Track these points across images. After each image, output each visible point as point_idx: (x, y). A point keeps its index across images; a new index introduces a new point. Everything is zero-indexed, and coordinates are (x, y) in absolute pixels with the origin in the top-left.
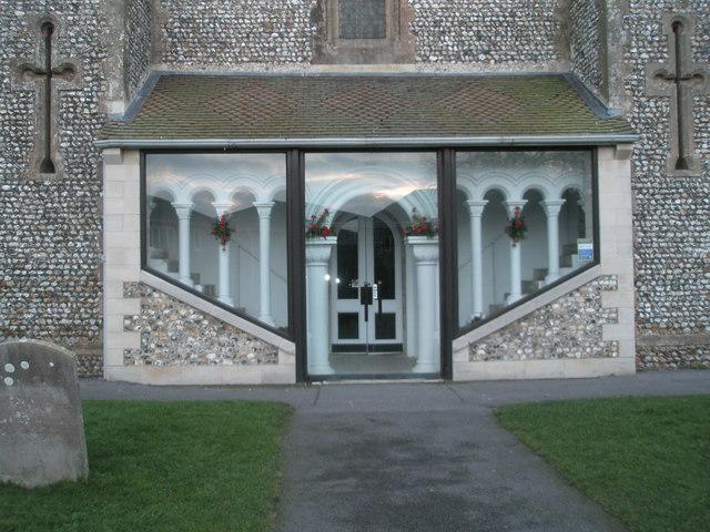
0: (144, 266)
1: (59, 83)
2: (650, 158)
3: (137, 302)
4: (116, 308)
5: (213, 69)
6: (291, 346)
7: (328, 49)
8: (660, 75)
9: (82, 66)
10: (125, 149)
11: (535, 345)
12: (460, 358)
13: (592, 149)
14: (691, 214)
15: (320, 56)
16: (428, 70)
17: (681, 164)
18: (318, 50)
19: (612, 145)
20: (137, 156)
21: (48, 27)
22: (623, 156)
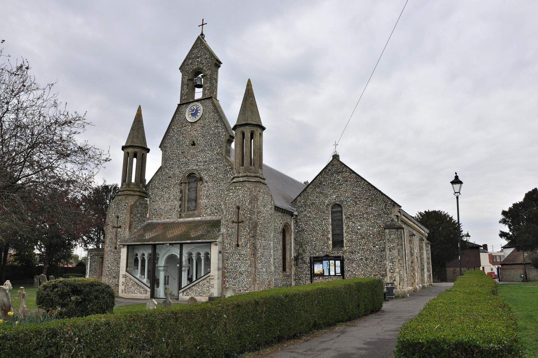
0: (127, 271)
1: (119, 229)
2: (230, 244)
4: (122, 280)
5: (159, 221)
6: (149, 290)
7: (183, 215)
8: (233, 222)
10: (124, 245)
11: (196, 293)
12: (181, 295)
13: (210, 243)
14: (239, 259)
15: (181, 217)
16: (204, 219)
18: (180, 215)
19: (213, 242)
21: (118, 217)
22: (216, 245)
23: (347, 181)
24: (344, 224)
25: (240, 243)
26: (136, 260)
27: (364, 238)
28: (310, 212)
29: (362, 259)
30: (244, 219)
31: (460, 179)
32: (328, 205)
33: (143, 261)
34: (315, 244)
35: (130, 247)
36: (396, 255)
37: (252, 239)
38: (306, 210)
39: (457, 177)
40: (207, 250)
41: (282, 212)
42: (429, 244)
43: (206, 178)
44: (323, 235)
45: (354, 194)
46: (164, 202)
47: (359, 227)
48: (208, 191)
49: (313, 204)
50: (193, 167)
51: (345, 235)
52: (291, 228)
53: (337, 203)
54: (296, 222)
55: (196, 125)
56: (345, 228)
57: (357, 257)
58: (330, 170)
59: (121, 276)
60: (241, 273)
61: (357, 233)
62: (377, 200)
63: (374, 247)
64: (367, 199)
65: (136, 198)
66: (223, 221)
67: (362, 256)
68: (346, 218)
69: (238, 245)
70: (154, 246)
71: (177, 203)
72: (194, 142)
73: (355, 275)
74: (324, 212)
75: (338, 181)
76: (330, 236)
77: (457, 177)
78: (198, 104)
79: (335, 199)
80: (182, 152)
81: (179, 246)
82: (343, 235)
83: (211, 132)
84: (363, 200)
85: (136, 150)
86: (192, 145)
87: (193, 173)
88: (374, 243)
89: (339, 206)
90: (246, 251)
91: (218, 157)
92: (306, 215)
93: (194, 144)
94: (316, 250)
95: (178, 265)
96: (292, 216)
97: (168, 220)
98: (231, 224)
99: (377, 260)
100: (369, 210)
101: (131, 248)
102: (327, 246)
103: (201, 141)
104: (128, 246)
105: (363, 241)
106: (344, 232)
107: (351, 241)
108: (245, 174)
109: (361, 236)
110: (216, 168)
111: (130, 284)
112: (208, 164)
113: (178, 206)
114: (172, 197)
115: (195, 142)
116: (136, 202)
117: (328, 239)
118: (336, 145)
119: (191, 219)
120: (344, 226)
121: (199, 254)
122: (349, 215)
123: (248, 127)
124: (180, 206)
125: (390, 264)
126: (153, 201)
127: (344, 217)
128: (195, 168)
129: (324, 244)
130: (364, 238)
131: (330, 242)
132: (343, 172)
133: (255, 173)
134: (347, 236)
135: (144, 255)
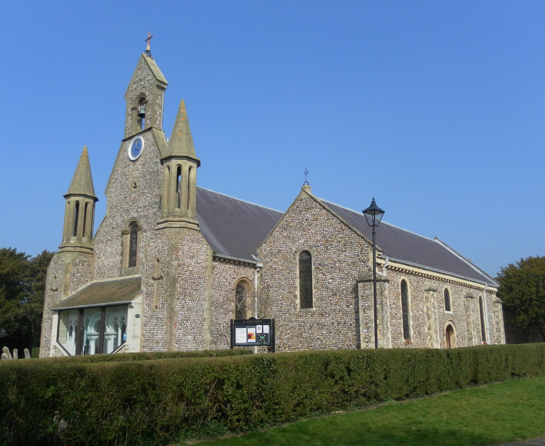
3: (54, 350)
5: (103, 281)
7: (123, 272)
9: (59, 289)
10: (55, 311)
15: (121, 275)
20: (57, 312)
23: (316, 220)
24: (313, 276)
27: (336, 295)
28: (276, 263)
29: (333, 323)
30: (163, 275)
31: (379, 205)
32: (296, 252)
34: (281, 304)
35: (62, 312)
37: (169, 299)
38: (271, 260)
39: (373, 203)
41: (235, 265)
42: (498, 302)
43: (145, 227)
44: (289, 293)
45: (325, 237)
46: (108, 257)
47: (330, 281)
48: (146, 242)
49: (280, 251)
51: (314, 291)
52: (253, 284)
53: (306, 249)
54: (261, 276)
55: (138, 163)
56: (314, 282)
57: (327, 320)
58: (297, 207)
60: (157, 342)
61: (328, 288)
62: (351, 243)
64: (340, 242)
65: (76, 254)
66: (143, 278)
68: (316, 268)
71: (119, 258)
73: (326, 344)
74: (291, 262)
75: (306, 220)
76: (298, 293)
77: (373, 203)
78: (141, 137)
79: (303, 245)
82: (312, 291)
83: (151, 170)
87: (134, 222)
88: (348, 301)
89: (307, 253)
90: (163, 314)
94: (281, 311)
96: (256, 268)
97: (110, 279)
98: (152, 281)
99: (351, 325)
100: (342, 257)
102: (294, 306)
103: (141, 183)
105: (335, 300)
106: (313, 286)
110: (154, 214)
112: (148, 209)
116: (74, 260)
117: (295, 296)
118: (306, 173)
119: (130, 277)
120: (313, 280)
122: (319, 264)
123: (173, 160)
125: (365, 330)
126: (98, 258)
127: (313, 267)
128: (136, 215)
129: (291, 304)
130: (336, 295)
131: (298, 301)
132: (312, 208)
133: (180, 217)
134: (316, 292)
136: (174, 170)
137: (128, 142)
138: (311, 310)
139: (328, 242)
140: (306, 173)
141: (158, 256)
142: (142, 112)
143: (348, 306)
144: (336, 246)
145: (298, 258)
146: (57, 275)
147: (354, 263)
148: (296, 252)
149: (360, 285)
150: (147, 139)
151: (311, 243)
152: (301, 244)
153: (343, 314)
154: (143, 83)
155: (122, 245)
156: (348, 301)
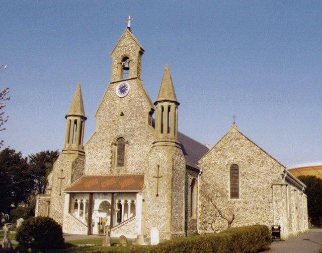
10: (67, 193)
12: (112, 233)
17: (157, 195)
19: (138, 192)
22: (141, 194)
23: (242, 146)
25: (159, 194)
26: (76, 205)
28: (213, 170)
32: (228, 165)
33: (82, 205)
36: (281, 206)
40: (133, 198)
41: (191, 169)
49: (215, 164)
50: (121, 133)
51: (240, 189)
53: (235, 163)
56: (240, 184)
57: (250, 206)
59: (64, 217)
60: (159, 217)
63: (264, 199)
67: (254, 206)
69: (157, 195)
70: (91, 194)
71: (109, 161)
72: (122, 113)
73: (248, 221)
76: (229, 189)
80: (113, 121)
81: (111, 195)
84: (255, 162)
85: (76, 118)
86: (121, 115)
88: (264, 196)
91: (141, 125)
92: (209, 172)
93: (122, 114)
95: (110, 210)
98: (152, 179)
100: (261, 169)
101: (72, 195)
104: (70, 193)
105: (255, 194)
107: (245, 194)
108: (164, 140)
109: (254, 190)
111: (72, 223)
113: (109, 163)
114: (104, 156)
115: (124, 113)
117: (227, 191)
121: (126, 201)
124: (111, 163)
128: (123, 133)
130: (256, 191)
135: (82, 201)
136: (166, 109)
137: (115, 84)
138: (238, 200)
139: (250, 161)
140: (234, 117)
141: (158, 163)
142: (126, 66)
143: (264, 199)
144: (256, 163)
145: (229, 168)
146: (64, 169)
147: (268, 174)
148: (228, 165)
149: (274, 186)
150: (132, 84)
151: (239, 160)
152: (231, 159)
153: (261, 203)
154: (127, 48)
155: (112, 152)
156: (264, 196)
